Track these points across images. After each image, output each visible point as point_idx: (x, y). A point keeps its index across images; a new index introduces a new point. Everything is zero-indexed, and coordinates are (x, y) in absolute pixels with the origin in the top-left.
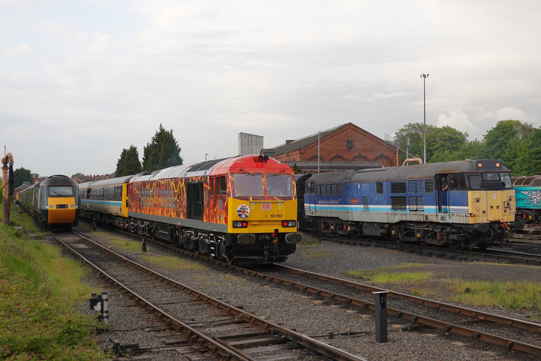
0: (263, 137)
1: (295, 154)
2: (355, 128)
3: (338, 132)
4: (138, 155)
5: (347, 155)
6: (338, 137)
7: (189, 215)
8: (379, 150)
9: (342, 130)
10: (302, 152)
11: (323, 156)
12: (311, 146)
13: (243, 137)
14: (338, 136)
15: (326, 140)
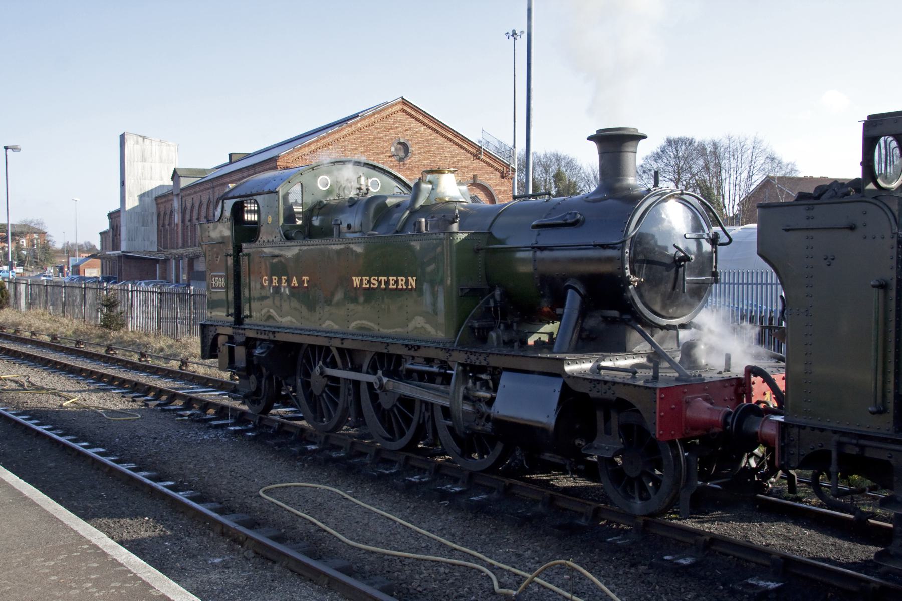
6: (373, 132)
8: (467, 168)
14: (372, 129)
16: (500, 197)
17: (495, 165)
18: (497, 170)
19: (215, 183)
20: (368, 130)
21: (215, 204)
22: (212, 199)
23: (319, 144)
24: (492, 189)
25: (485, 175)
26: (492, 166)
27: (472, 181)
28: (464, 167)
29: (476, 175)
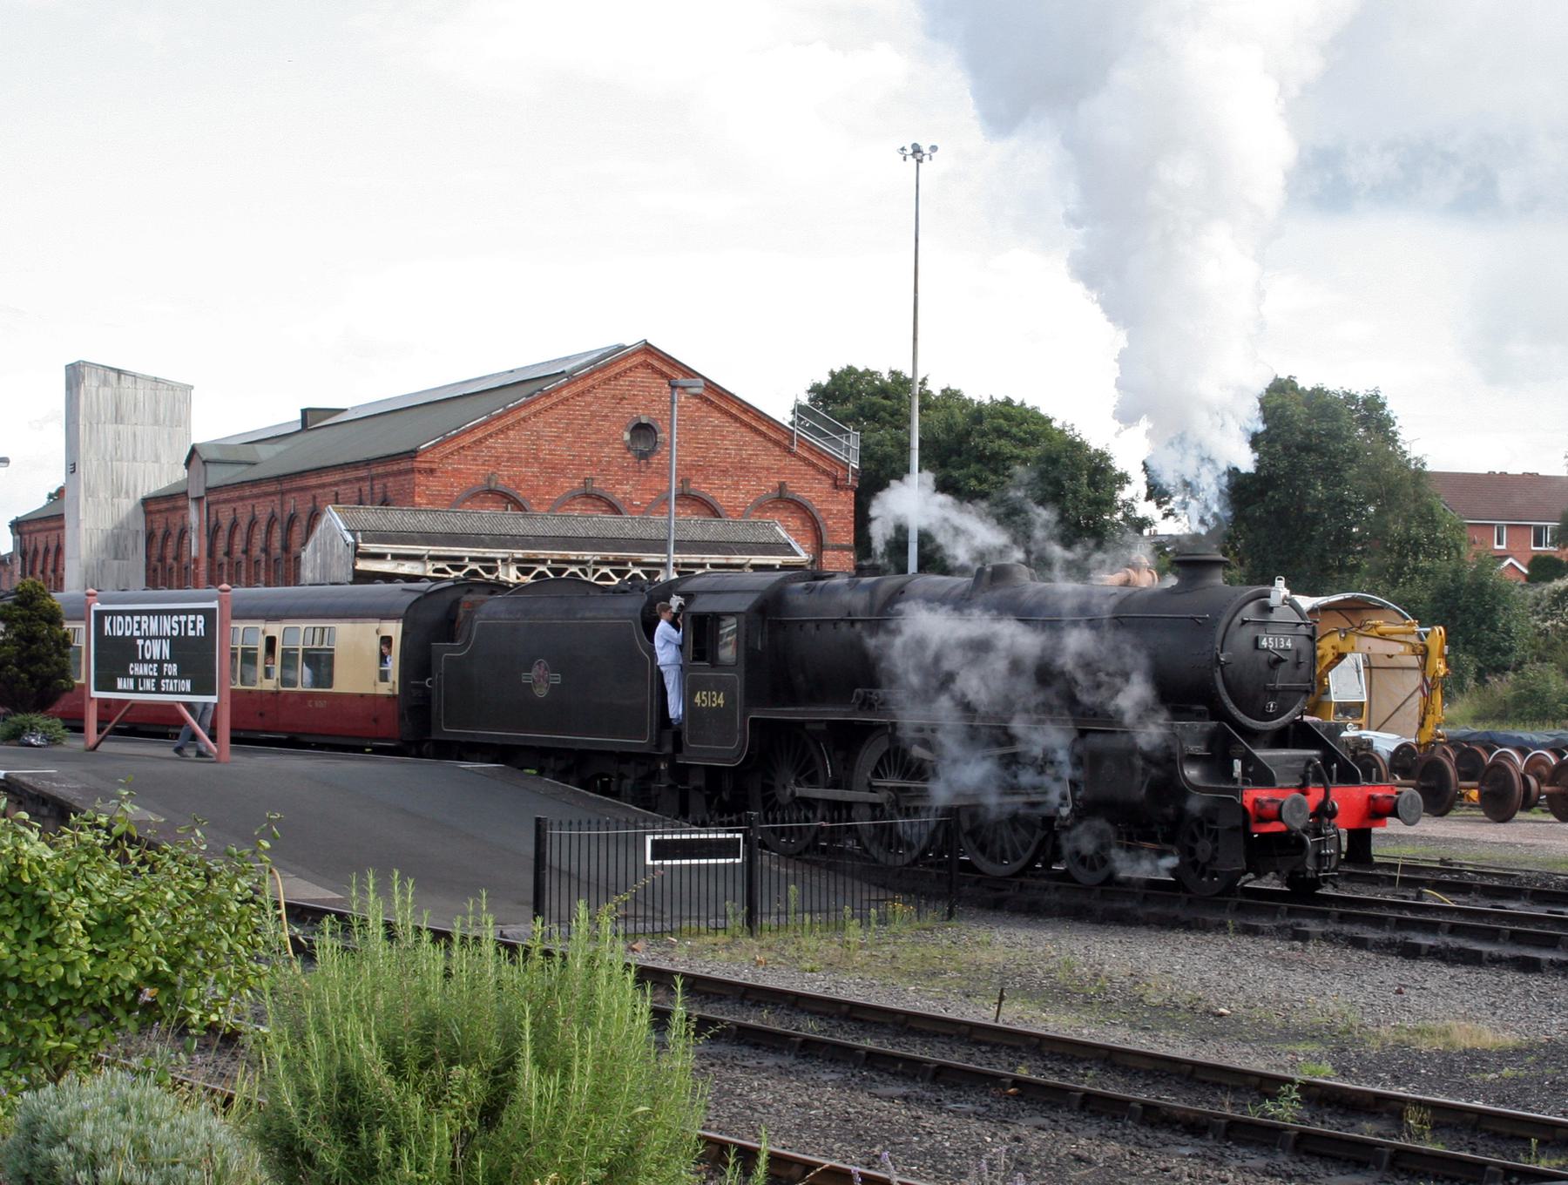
1: (386, 475)
2: (665, 369)
5: (627, 488)
6: (590, 405)
8: (768, 469)
10: (427, 465)
12: (468, 440)
14: (589, 398)
16: (830, 522)
17: (820, 463)
18: (825, 472)
19: (286, 486)
20: (580, 402)
21: (285, 525)
22: (279, 515)
23: (491, 429)
24: (816, 506)
25: (802, 483)
26: (814, 465)
27: (776, 494)
28: (763, 468)
29: (784, 483)
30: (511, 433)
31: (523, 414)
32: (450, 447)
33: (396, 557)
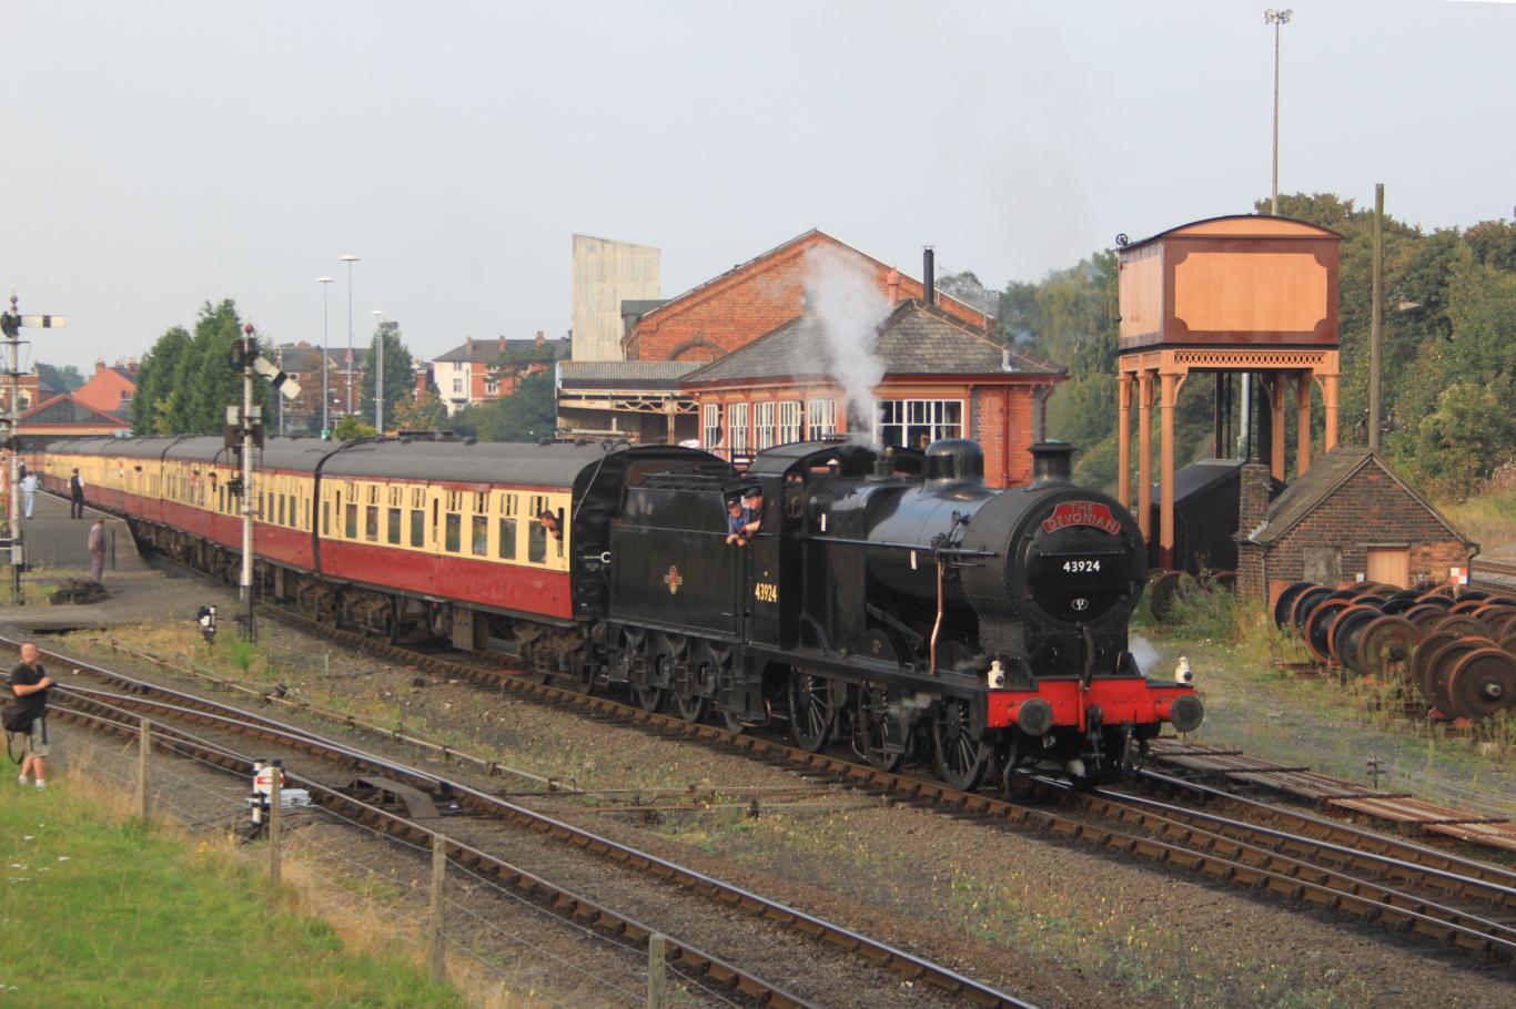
0: (659, 251)
3: (772, 262)
4: (235, 308)
7: (348, 535)
9: (788, 254)
10: (648, 328)
11: (723, 340)
13: (582, 250)
15: (732, 287)
23: (696, 300)
30: (713, 302)
31: (721, 288)
32: (664, 315)
33: (588, 397)
